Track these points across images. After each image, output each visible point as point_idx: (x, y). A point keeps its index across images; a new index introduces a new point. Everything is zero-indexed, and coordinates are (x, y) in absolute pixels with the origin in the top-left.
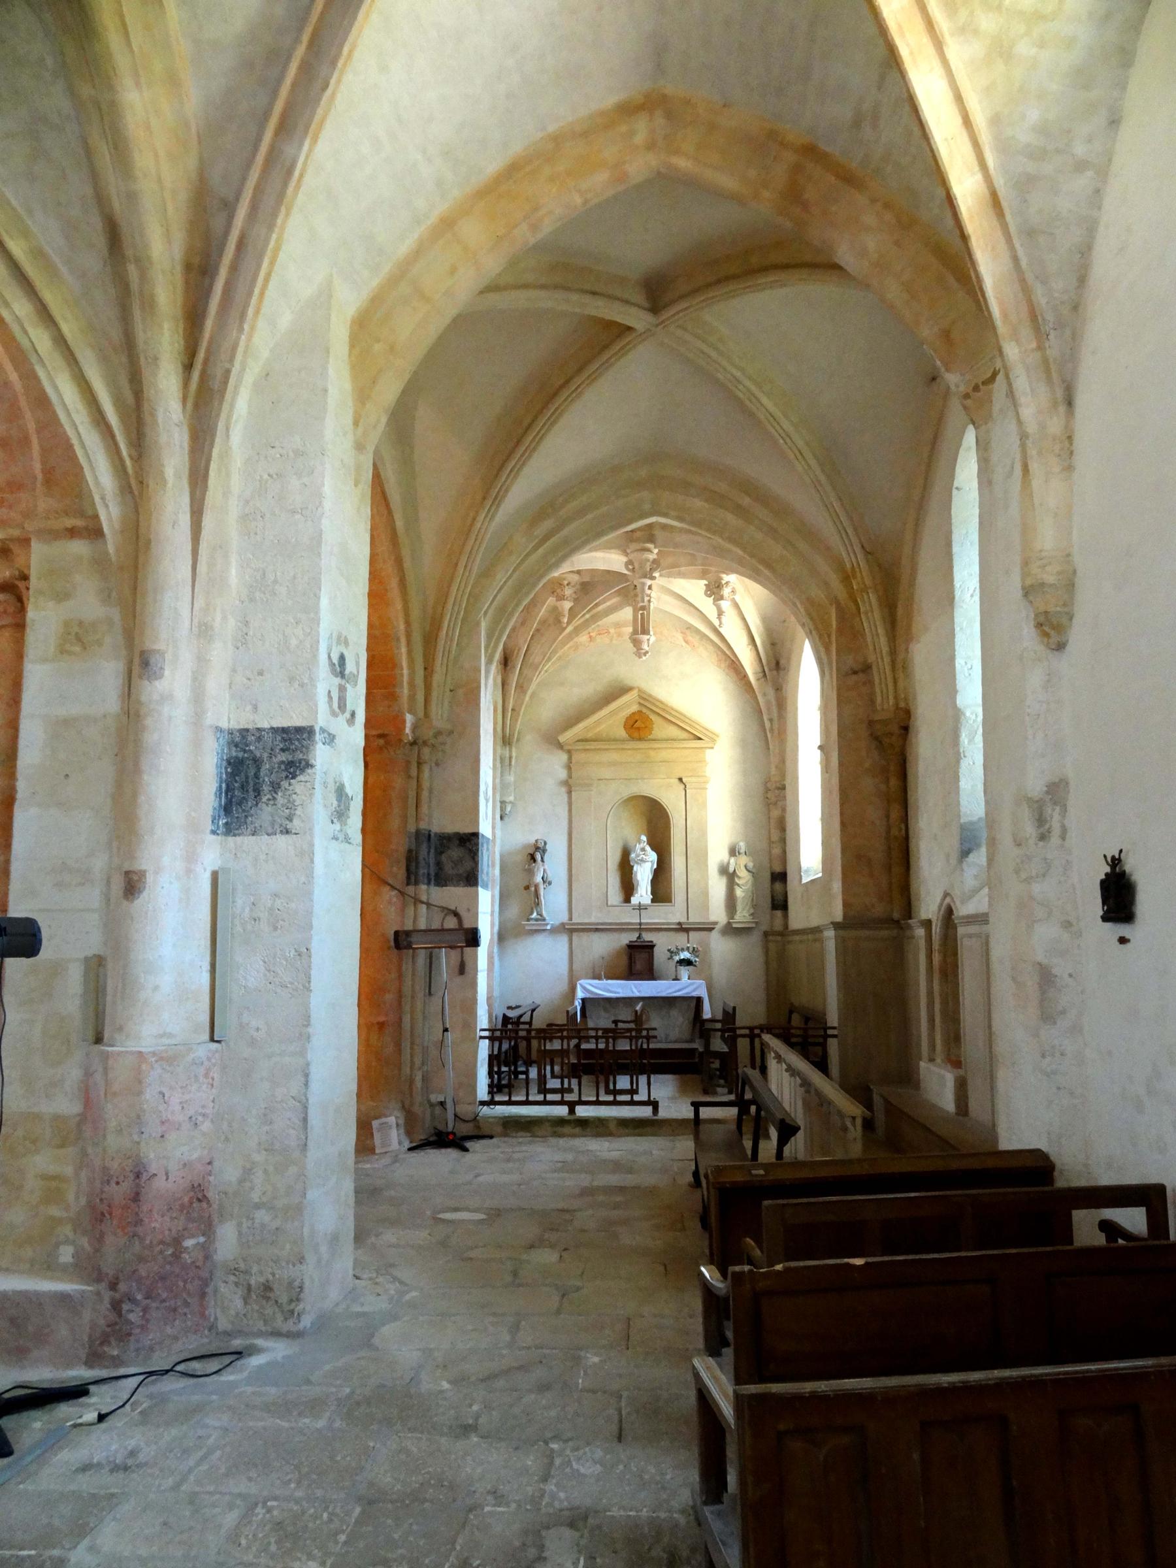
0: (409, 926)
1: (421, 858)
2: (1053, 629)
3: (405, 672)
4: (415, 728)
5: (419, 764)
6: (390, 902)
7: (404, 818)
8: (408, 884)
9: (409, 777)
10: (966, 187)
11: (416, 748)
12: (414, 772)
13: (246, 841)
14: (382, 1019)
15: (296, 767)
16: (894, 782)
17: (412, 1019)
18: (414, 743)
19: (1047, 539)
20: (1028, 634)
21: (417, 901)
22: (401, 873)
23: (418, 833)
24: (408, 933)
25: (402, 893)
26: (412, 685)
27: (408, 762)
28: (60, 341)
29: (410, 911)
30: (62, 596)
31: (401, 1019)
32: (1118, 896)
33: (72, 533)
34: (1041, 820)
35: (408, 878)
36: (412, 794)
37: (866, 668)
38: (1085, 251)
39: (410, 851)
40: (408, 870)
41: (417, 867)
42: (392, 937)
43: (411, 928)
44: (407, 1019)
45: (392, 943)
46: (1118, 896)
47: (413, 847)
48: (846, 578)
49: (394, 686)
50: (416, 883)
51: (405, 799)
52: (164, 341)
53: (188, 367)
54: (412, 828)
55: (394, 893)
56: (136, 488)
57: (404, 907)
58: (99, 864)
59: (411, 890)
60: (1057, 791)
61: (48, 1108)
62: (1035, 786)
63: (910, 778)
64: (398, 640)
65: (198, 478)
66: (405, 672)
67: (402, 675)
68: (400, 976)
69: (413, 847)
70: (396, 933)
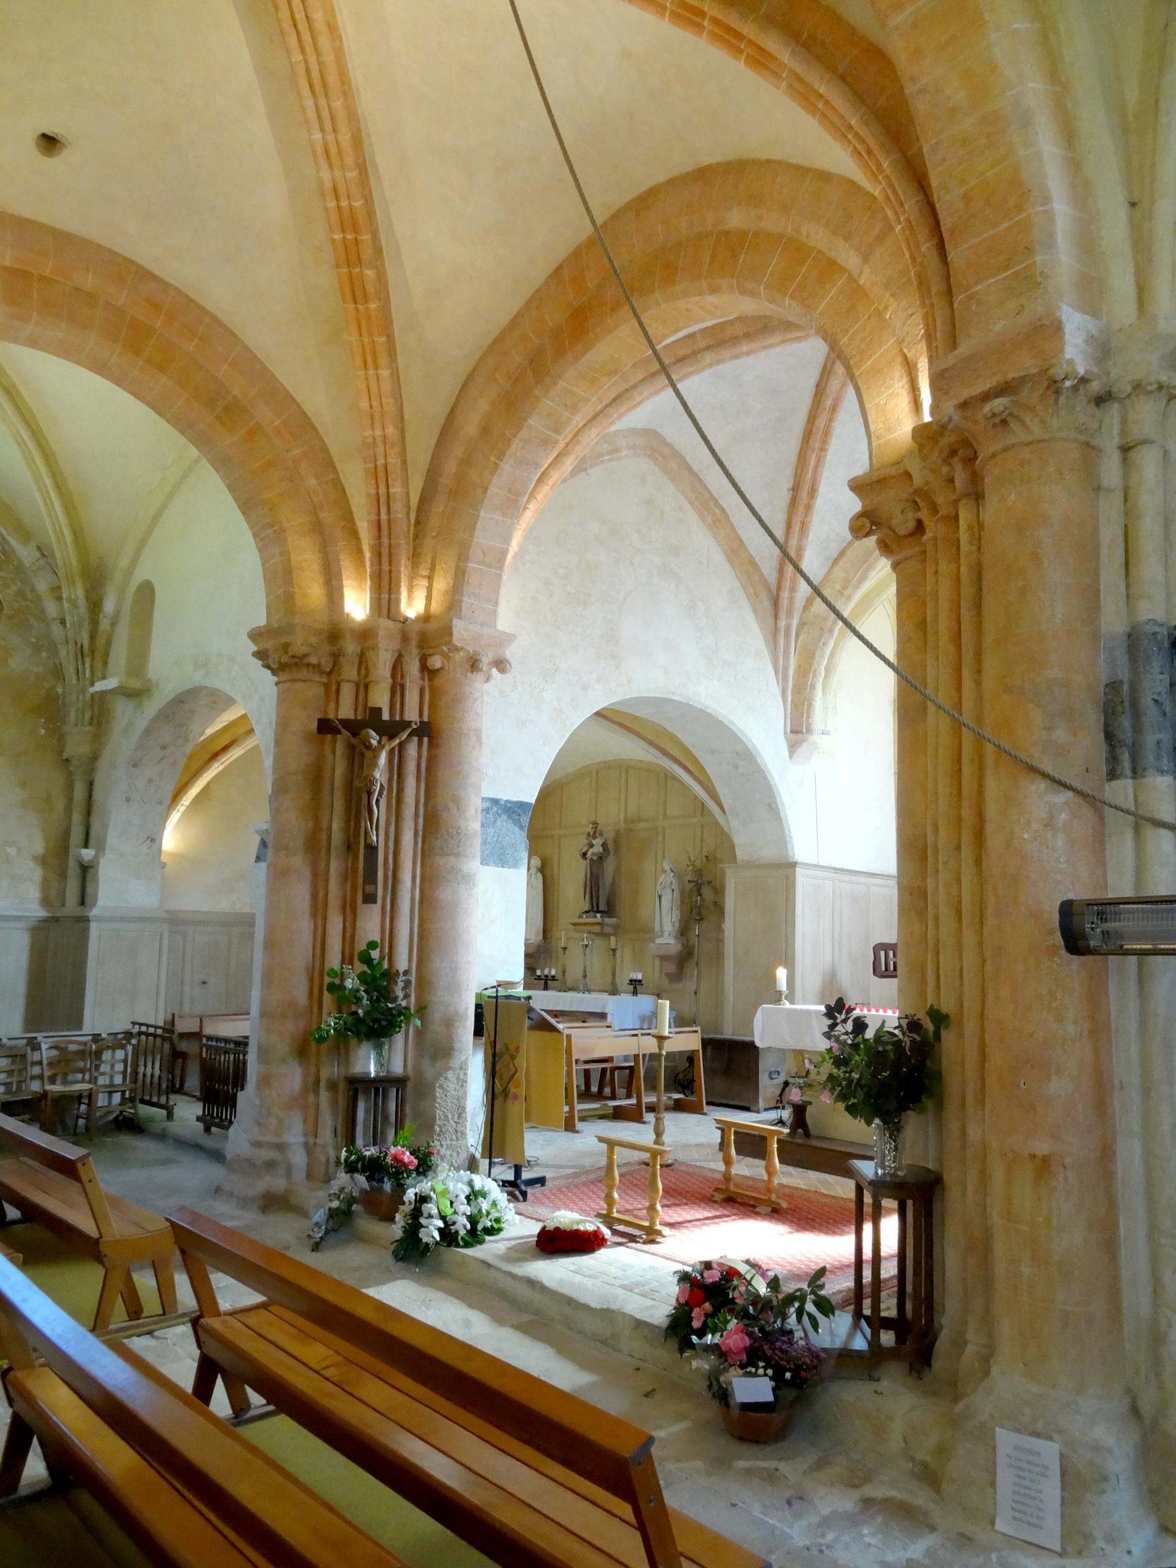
0: (1121, 886)
1: (1147, 701)
3: (1062, 210)
4: (1103, 349)
5: (1126, 450)
6: (1049, 824)
7: (1091, 597)
8: (1112, 775)
9: (1098, 489)
11: (1114, 409)
12: (1111, 470)
14: (1042, 1147)
17: (1148, 1154)
18: (1101, 400)
21: (1142, 821)
22: (1086, 743)
23: (1134, 640)
24: (1104, 908)
25: (1093, 801)
26: (1088, 245)
27: (1090, 450)
29: (1122, 847)
31: (1107, 1154)
35: (1113, 759)
36: (1110, 533)
39: (1113, 686)
40: (1109, 736)
41: (1137, 728)
42: (1056, 917)
43: (1129, 893)
44: (1130, 1154)
45: (1058, 939)
47: (1124, 674)
49: (1029, 250)
50: (1137, 772)
51: (1088, 553)
54: (1113, 621)
55: (1063, 797)
57: (1100, 840)
59: (1121, 791)
64: (1026, 123)
66: (1062, 210)
67: (1049, 216)
68: (1099, 1030)
69: (1124, 674)
70: (1067, 910)
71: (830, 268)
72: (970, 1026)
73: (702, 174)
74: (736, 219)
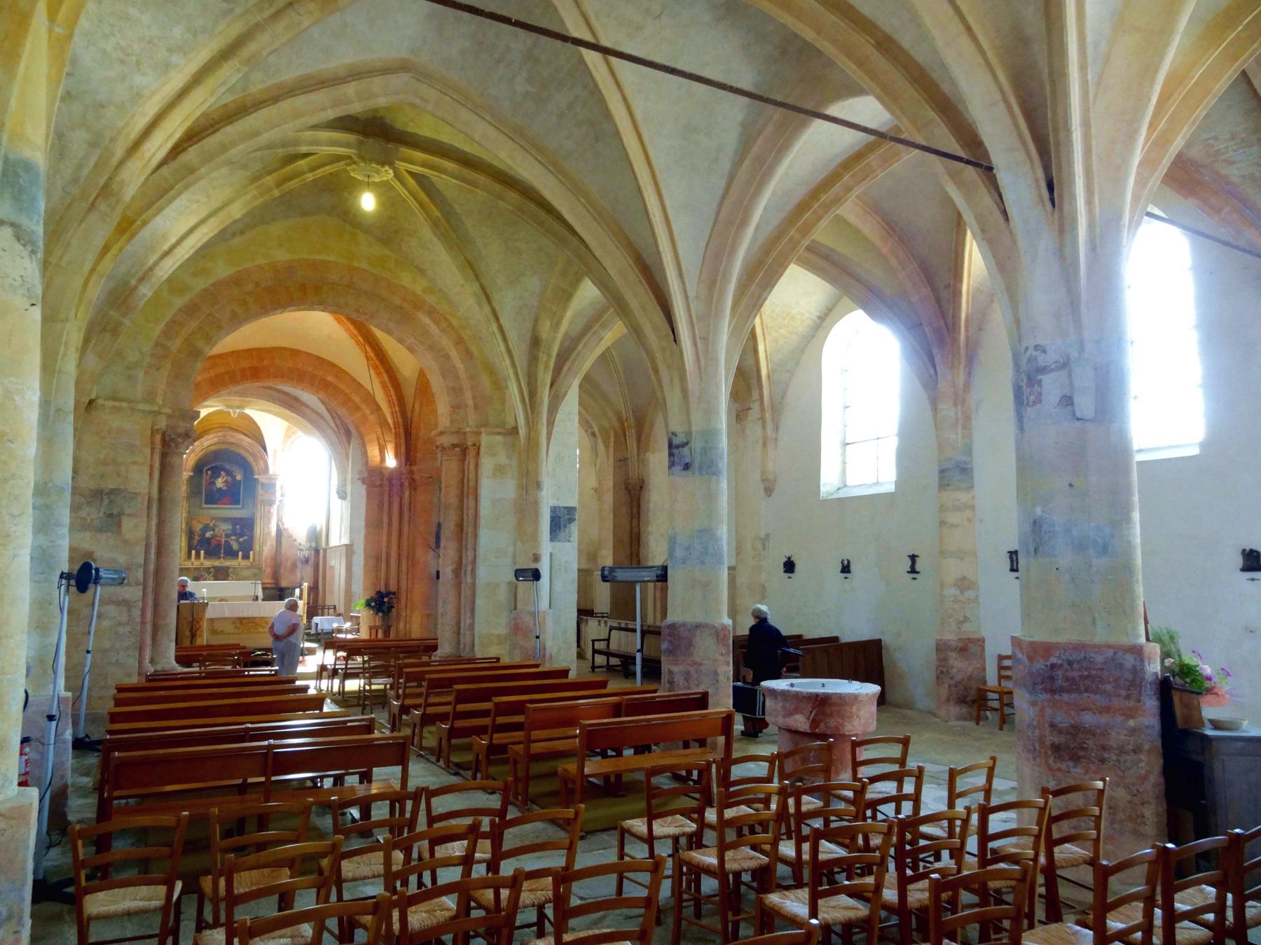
2: (769, 491)
10: (764, 372)
13: (558, 544)
15: (571, 520)
16: (635, 510)
19: (770, 467)
20: (762, 493)
28: (517, 375)
30: (494, 455)
32: (789, 566)
33: (499, 433)
34: (764, 544)
37: (625, 460)
38: (785, 391)
46: (789, 566)
48: (621, 421)
52: (545, 378)
53: (552, 385)
56: (531, 424)
58: (511, 549)
60: (767, 536)
61: (495, 632)
62: (763, 536)
63: (643, 508)
65: (551, 423)
71: (357, 408)
72: (404, 594)
73: (318, 358)
74: (330, 378)
